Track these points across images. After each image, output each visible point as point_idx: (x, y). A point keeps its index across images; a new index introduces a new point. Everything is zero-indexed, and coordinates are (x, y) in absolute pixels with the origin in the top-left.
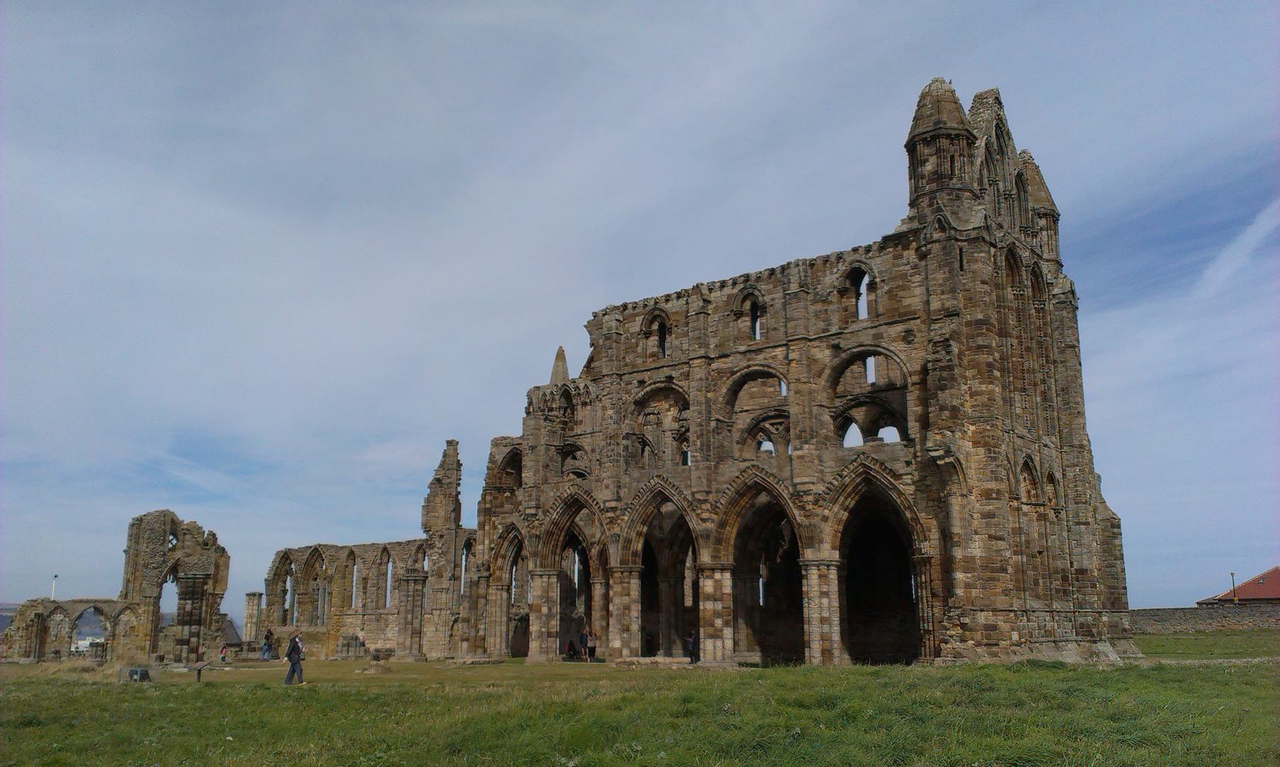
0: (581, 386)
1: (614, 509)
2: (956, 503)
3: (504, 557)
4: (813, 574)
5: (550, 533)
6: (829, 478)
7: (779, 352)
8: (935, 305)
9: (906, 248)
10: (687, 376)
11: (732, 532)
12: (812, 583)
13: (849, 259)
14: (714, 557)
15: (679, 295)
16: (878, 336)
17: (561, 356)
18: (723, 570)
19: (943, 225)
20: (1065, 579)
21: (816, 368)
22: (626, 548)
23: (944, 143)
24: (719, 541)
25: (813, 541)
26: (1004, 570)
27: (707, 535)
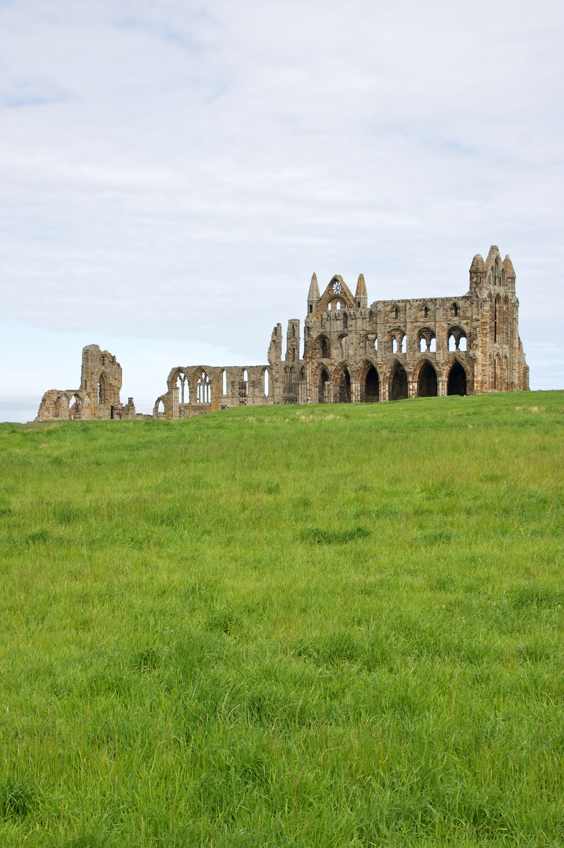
0: (352, 312)
1: (381, 364)
2: (475, 367)
3: (317, 375)
4: (441, 384)
5: (358, 370)
6: (445, 359)
7: (433, 323)
8: (474, 317)
9: (468, 300)
10: (405, 326)
11: (418, 372)
12: (440, 386)
13: (454, 300)
14: (413, 379)
15: (403, 301)
16: (460, 323)
17: (314, 277)
18: (415, 382)
19: (477, 297)
20: (508, 385)
21: (443, 329)
22: (384, 376)
23: (479, 274)
24: (414, 374)
25: (440, 375)
26: (486, 383)
27: (410, 373)
